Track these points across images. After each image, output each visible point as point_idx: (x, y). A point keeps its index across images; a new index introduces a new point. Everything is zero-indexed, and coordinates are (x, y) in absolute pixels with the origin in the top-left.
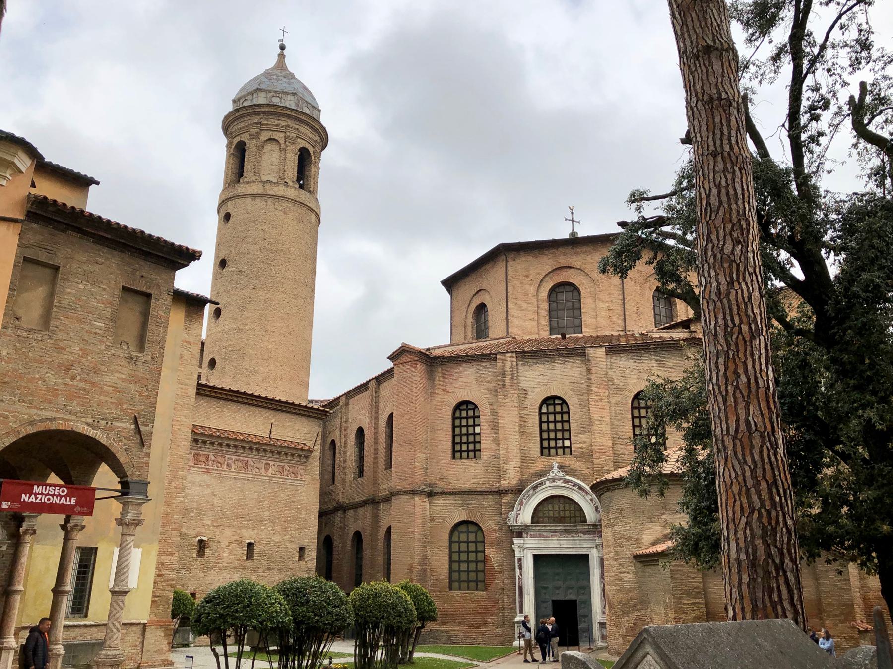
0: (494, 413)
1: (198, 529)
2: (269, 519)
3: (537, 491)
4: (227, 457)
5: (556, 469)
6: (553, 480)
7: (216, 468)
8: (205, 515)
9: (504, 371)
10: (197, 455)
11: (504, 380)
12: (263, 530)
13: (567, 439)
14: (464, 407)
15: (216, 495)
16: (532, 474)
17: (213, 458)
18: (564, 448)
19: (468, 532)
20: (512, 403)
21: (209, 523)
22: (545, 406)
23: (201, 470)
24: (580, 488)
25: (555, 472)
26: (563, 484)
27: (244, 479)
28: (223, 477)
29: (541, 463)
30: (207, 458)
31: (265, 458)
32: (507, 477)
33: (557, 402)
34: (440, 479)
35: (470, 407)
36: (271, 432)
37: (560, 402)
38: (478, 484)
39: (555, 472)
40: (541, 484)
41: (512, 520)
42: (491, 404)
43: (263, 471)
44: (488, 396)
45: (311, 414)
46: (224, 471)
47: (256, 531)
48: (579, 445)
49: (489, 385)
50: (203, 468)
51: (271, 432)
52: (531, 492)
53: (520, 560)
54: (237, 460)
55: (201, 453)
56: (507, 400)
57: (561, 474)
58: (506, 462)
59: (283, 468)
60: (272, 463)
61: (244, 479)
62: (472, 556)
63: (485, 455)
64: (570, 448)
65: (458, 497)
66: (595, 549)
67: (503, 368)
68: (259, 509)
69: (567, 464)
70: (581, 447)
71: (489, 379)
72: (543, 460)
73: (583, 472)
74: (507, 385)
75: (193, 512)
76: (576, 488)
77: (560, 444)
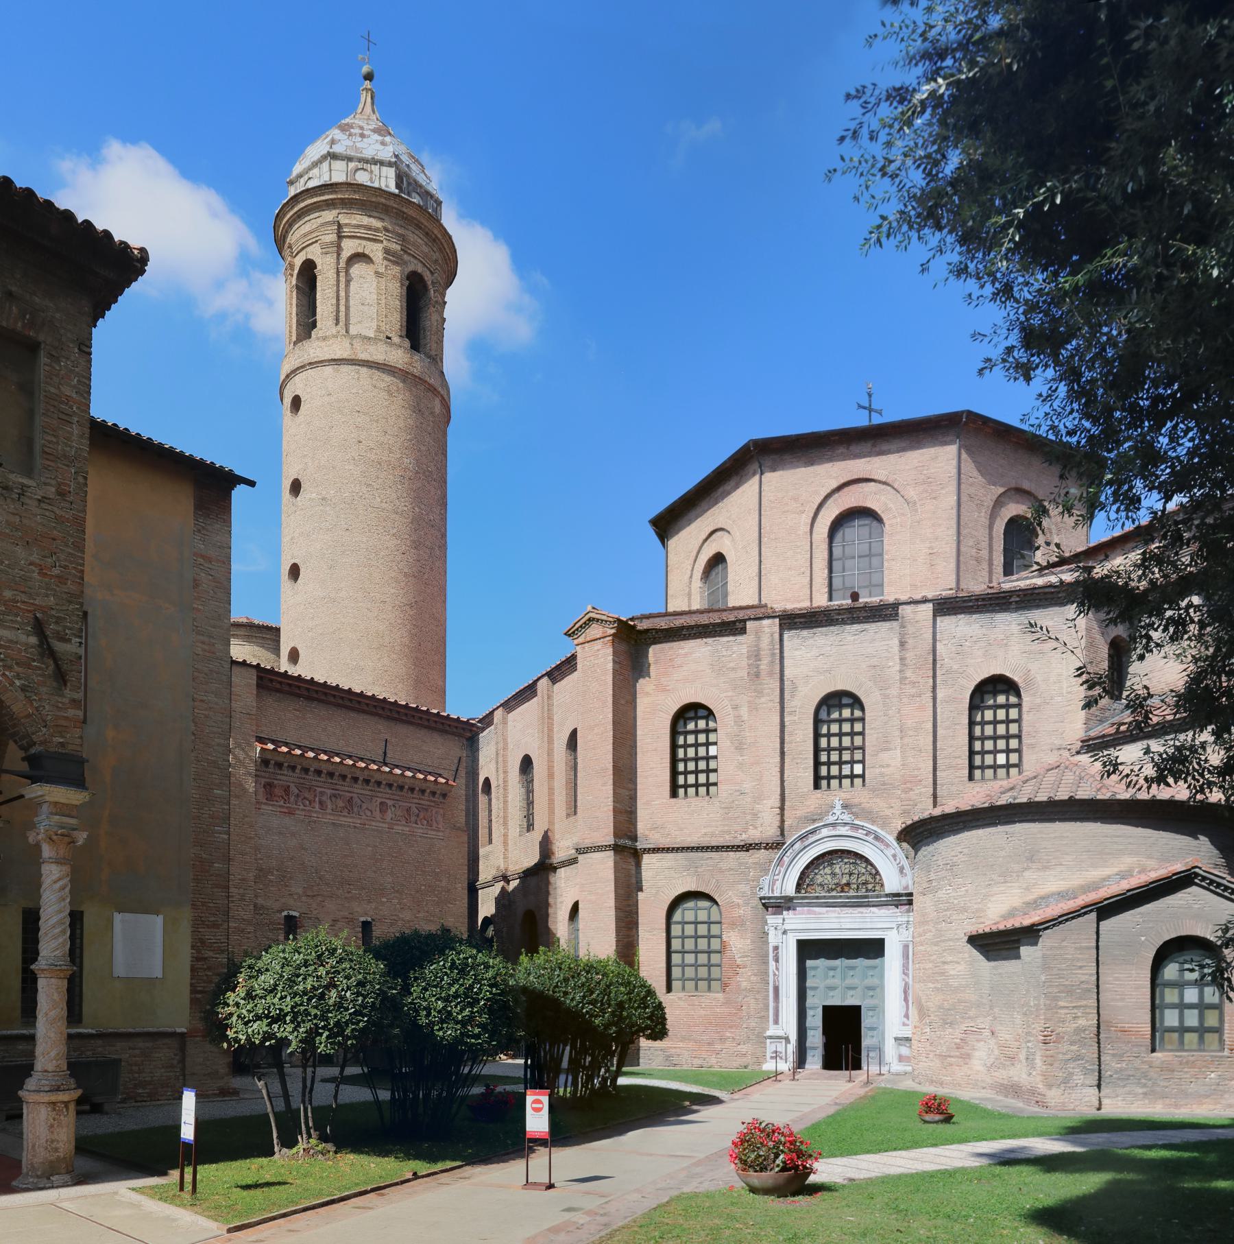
0: (739, 721)
1: (283, 900)
3: (807, 843)
4: (319, 790)
5: (838, 810)
6: (834, 825)
8: (291, 878)
9: (759, 650)
11: (758, 667)
13: (858, 762)
14: (692, 714)
16: (800, 818)
18: (852, 776)
19: (697, 909)
20: (770, 704)
21: (300, 891)
22: (824, 708)
24: (877, 838)
25: (838, 813)
26: (849, 833)
27: (349, 826)
28: (315, 822)
29: (816, 799)
31: (379, 795)
32: (759, 823)
33: (845, 701)
34: (651, 829)
35: (702, 712)
36: (385, 753)
37: (850, 701)
38: (713, 835)
39: (838, 813)
40: (813, 832)
41: (766, 888)
42: (736, 707)
43: (377, 814)
44: (730, 694)
46: (316, 812)
48: (877, 771)
49: (732, 675)
51: (385, 753)
52: (798, 846)
53: (776, 948)
54: (335, 796)
56: (763, 700)
57: (847, 818)
58: (758, 799)
62: (703, 944)
63: (723, 791)
64: (863, 776)
65: (680, 855)
66: (895, 931)
67: (757, 646)
69: (856, 801)
70: (882, 775)
71: (732, 665)
72: (819, 795)
73: (882, 814)
74: (763, 674)
76: (870, 838)
77: (846, 770)
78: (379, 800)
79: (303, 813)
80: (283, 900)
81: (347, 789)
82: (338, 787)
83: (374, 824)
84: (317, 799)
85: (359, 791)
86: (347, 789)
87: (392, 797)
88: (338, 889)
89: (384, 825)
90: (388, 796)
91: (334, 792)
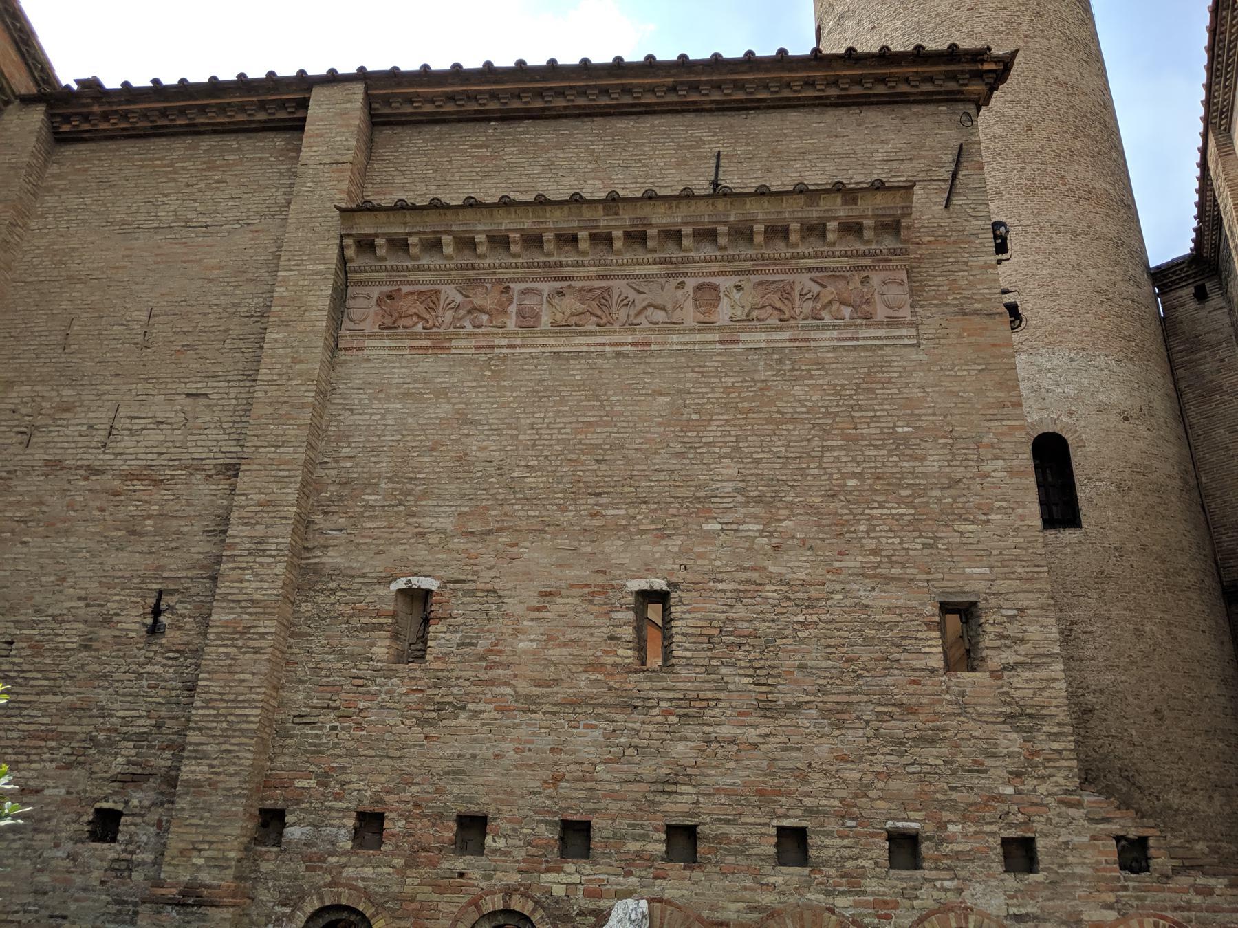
1: (397, 551)
2: (742, 491)
4: (517, 287)
7: (469, 328)
8: (425, 495)
10: (390, 297)
12: (709, 536)
15: (478, 422)
17: (459, 298)
21: (447, 523)
23: (408, 343)
27: (602, 355)
28: (504, 359)
30: (431, 299)
31: (690, 268)
43: (689, 315)
45: (904, 88)
47: (674, 544)
50: (415, 336)
54: (560, 293)
55: (406, 289)
59: (786, 293)
60: (725, 283)
61: (602, 355)
68: (681, 455)
75: (375, 488)
78: (691, 283)
79: (473, 342)
80: (397, 551)
81: (593, 271)
82: (566, 271)
83: (675, 338)
84: (513, 308)
85: (628, 270)
86: (593, 271)
87: (730, 267)
88: (562, 509)
89: (709, 337)
90: (715, 267)
91: (558, 285)
